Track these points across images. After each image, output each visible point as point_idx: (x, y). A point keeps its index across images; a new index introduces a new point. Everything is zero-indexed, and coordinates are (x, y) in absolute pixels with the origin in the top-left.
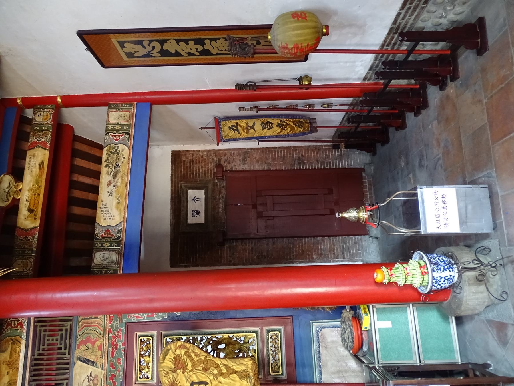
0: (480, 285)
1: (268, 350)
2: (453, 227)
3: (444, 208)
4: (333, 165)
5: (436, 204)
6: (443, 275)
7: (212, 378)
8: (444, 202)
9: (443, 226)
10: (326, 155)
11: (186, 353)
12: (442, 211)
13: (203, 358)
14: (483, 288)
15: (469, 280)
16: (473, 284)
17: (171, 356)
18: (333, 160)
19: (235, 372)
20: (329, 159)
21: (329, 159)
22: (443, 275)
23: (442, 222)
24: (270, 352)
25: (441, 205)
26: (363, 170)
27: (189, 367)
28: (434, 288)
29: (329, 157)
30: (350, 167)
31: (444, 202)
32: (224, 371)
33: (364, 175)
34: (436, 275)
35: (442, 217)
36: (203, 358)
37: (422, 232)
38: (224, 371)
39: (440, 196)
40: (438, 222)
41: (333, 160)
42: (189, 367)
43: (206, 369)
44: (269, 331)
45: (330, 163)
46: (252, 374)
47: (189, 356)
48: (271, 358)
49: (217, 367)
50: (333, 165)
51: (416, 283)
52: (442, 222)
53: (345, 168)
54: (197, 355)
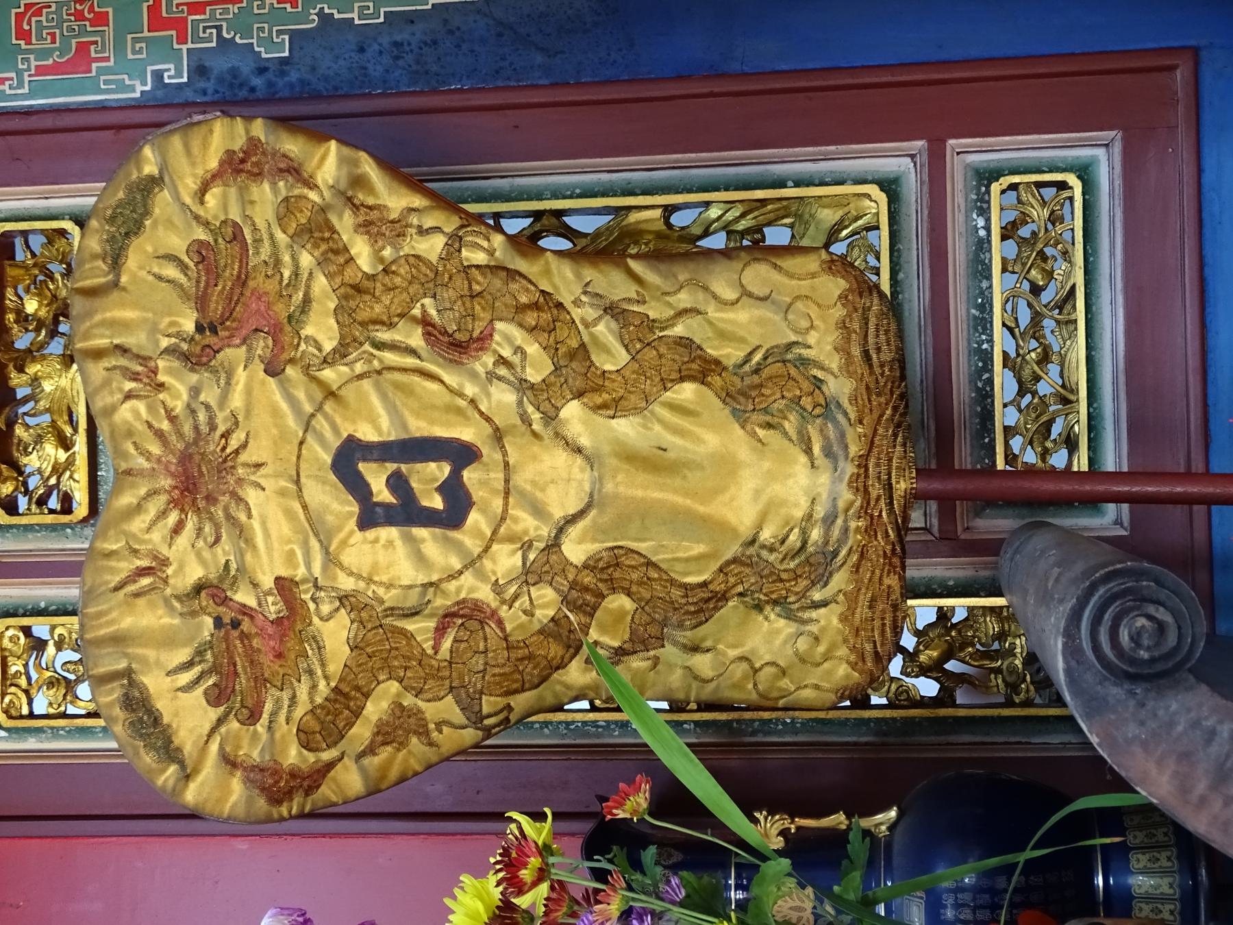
1: (983, 323)
7: (503, 398)
11: (287, 207)
13: (432, 247)
17: (168, 235)
19: (702, 368)
24: (1001, 342)
27: (322, 330)
32: (613, 357)
36: (432, 247)
38: (613, 357)
42: (322, 330)
43: (456, 346)
44: (987, 176)
46: (840, 387)
47: (317, 231)
48: (1004, 384)
49: (546, 313)
54: (374, 225)
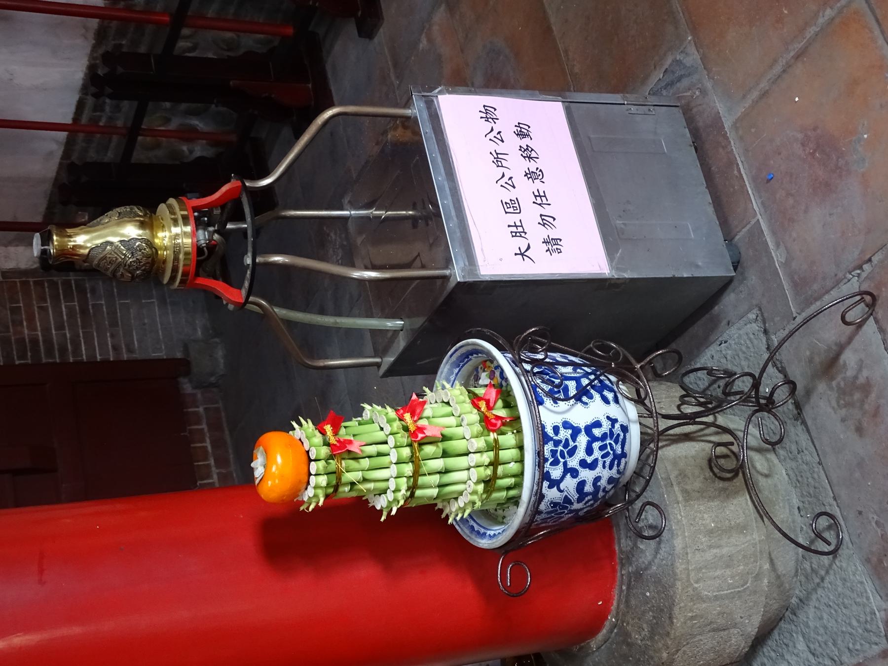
0: (727, 495)
2: (582, 253)
3: (530, 175)
4: (50, 351)
5: (498, 159)
6: (581, 414)
8: (528, 153)
9: (538, 250)
10: (15, 311)
12: (525, 190)
14: (740, 507)
15: (683, 475)
16: (702, 494)
18: (46, 330)
20: (32, 327)
21: (32, 327)
22: (581, 414)
23: (536, 234)
25: (517, 165)
26: (178, 368)
28: (552, 494)
29: (31, 319)
30: (125, 357)
31: (528, 153)
33: (187, 387)
34: (552, 414)
35: (530, 215)
37: (458, 273)
39: (506, 125)
40: (518, 231)
41: (46, 330)
45: (34, 342)
50: (50, 351)
51: (463, 485)
52: (536, 234)
53: (105, 363)
